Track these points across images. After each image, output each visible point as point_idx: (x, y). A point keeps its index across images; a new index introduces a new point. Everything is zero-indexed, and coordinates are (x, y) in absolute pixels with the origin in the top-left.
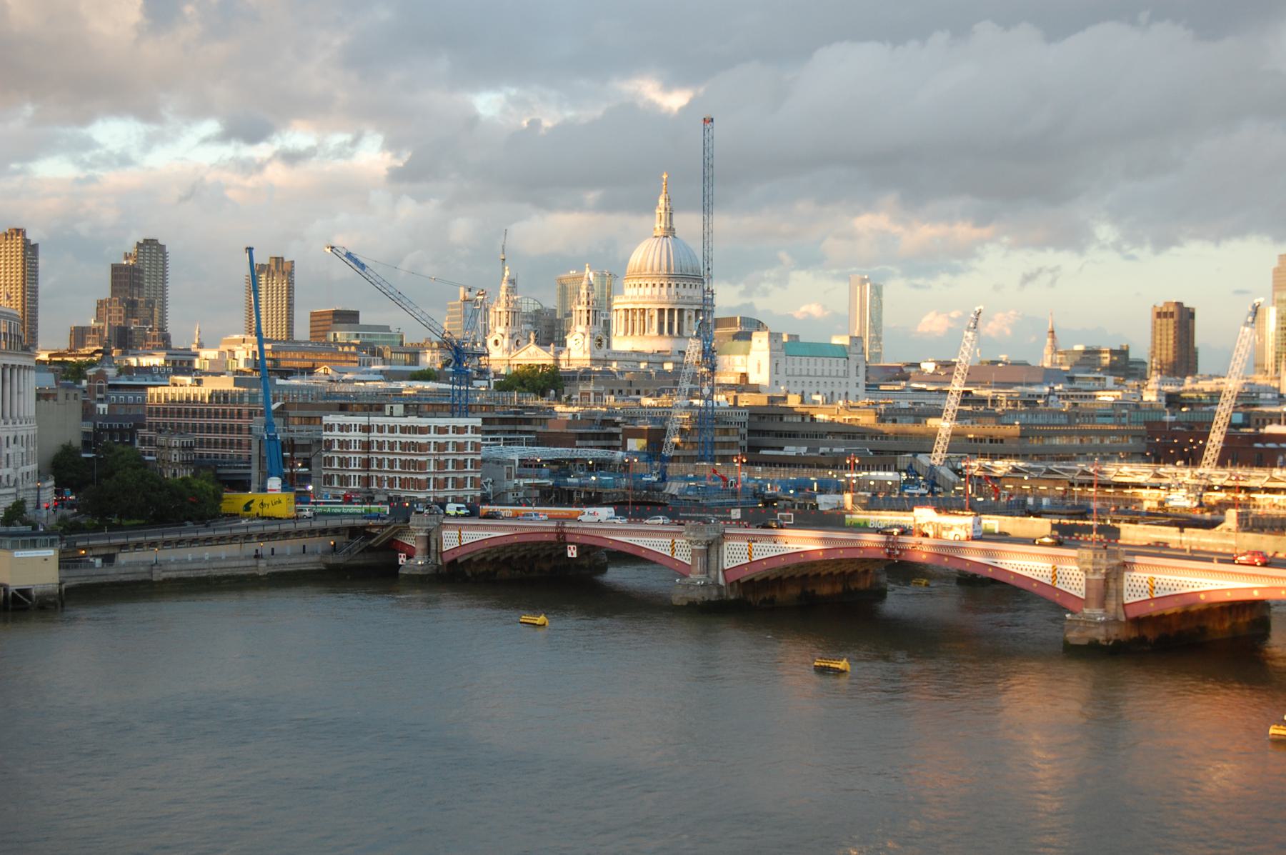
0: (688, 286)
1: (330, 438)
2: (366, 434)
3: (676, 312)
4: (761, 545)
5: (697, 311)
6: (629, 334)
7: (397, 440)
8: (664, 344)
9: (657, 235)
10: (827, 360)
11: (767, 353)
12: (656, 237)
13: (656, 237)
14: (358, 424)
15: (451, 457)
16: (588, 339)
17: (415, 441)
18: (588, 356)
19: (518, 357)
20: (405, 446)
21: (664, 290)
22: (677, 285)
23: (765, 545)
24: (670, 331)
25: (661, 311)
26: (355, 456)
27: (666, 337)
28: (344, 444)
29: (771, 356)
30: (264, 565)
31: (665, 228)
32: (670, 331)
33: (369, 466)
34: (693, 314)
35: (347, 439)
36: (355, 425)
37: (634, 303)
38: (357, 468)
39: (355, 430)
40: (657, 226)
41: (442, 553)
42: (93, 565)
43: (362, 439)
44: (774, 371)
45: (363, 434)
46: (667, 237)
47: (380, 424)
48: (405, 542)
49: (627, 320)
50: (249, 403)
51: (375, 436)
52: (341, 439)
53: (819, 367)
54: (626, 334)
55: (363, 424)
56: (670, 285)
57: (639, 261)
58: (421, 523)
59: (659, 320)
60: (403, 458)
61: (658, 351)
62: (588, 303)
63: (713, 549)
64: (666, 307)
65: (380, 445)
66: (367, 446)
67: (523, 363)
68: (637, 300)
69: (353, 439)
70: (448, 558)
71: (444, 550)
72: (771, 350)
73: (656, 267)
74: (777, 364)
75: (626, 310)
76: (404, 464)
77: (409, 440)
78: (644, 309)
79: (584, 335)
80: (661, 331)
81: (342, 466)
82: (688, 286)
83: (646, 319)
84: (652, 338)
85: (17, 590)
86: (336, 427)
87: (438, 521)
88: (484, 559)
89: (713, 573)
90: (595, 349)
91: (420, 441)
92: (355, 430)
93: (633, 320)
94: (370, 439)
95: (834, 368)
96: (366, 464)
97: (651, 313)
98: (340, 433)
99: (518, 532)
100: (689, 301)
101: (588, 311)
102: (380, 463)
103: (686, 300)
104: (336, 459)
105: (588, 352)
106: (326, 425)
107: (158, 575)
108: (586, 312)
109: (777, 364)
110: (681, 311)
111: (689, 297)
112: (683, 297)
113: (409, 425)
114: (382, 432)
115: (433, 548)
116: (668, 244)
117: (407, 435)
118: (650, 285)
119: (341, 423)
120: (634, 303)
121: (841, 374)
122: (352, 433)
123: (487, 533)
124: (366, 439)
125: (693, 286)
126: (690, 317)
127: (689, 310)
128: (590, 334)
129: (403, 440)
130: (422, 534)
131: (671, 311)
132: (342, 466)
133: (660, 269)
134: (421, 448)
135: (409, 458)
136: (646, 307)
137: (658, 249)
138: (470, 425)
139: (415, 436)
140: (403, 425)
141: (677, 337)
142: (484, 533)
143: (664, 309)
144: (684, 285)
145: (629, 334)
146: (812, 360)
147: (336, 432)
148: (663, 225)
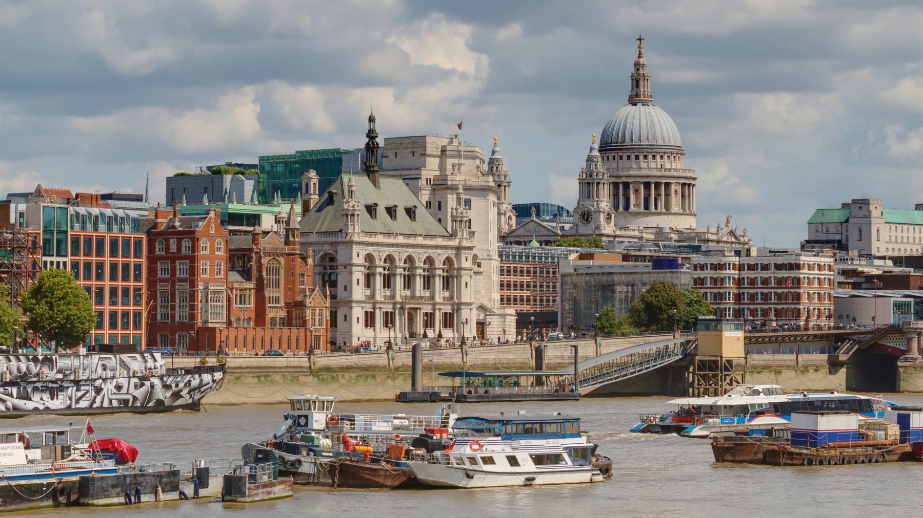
1: (702, 276)
3: (663, 186)
5: (684, 185)
25: (647, 185)
33: (740, 300)
34: (679, 188)
36: (729, 265)
39: (729, 269)
48: (888, 344)
51: (746, 274)
52: (715, 276)
65: (753, 282)
66: (739, 282)
69: (727, 276)
84: (637, 214)
85: (726, 360)
86: (709, 266)
94: (741, 277)
96: (738, 298)
98: (713, 272)
103: (673, 173)
110: (667, 185)
112: (669, 170)
113: (786, 262)
117: (784, 271)
119: (715, 263)
122: (728, 271)
126: (676, 191)
129: (780, 276)
146: (905, 227)
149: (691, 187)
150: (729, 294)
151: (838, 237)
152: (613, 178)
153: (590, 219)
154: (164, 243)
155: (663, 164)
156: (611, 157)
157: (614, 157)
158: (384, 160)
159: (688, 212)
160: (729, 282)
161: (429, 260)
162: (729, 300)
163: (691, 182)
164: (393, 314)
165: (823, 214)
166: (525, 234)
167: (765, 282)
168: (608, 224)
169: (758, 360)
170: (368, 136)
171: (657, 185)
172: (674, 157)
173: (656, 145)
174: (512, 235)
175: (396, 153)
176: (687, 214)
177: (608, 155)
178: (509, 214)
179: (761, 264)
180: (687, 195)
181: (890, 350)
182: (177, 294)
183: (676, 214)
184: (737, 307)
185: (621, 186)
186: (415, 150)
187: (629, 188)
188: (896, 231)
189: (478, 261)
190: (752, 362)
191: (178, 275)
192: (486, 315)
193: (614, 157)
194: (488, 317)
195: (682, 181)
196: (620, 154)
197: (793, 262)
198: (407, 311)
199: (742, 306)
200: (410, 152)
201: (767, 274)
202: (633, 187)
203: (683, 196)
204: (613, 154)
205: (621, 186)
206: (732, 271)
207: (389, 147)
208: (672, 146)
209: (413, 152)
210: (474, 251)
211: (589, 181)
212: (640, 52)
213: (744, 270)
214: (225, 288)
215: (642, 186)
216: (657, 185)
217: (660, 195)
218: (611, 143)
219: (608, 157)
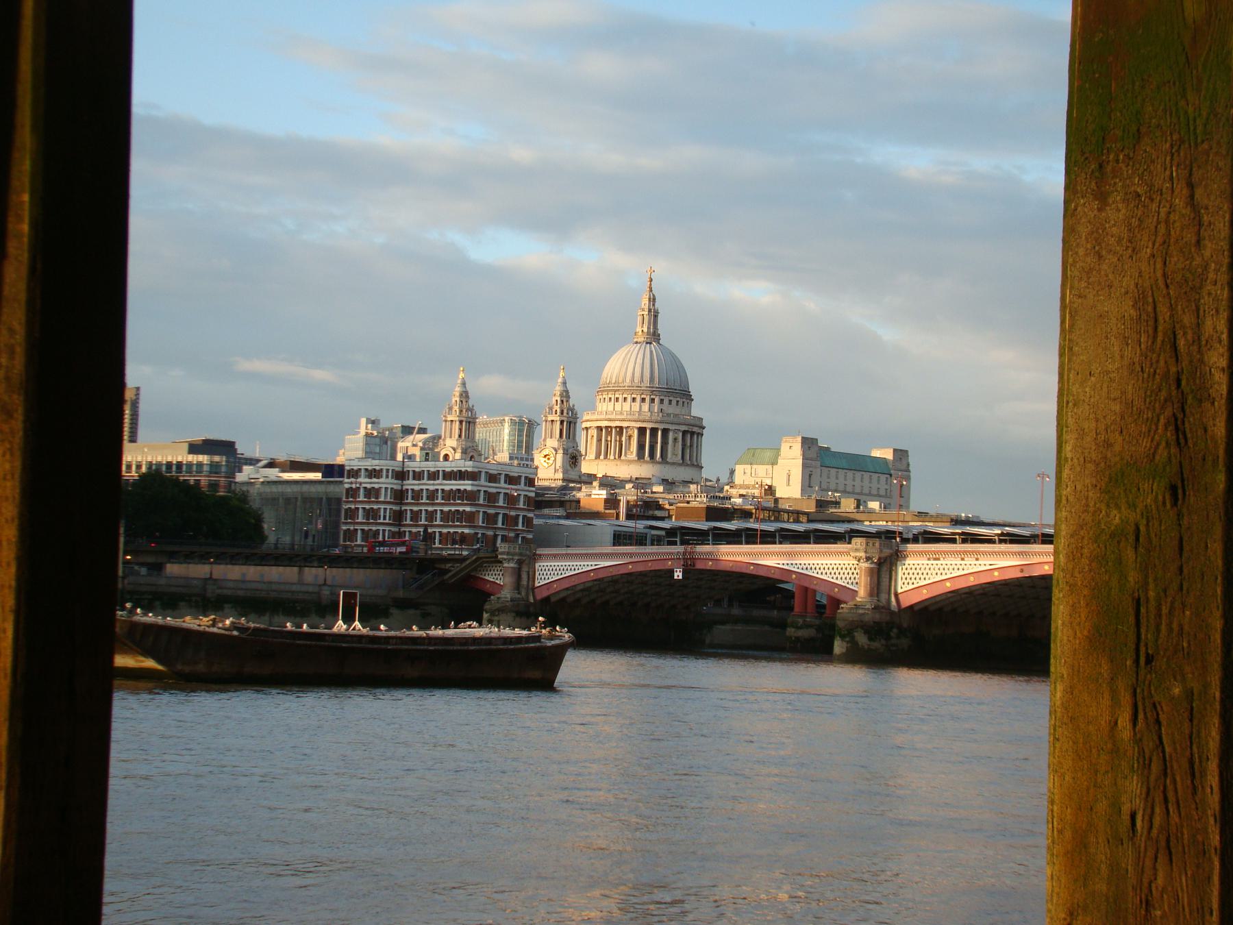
0: (674, 402)
2: (400, 482)
3: (660, 433)
4: (944, 562)
5: (684, 433)
6: (602, 457)
7: (440, 487)
8: (643, 470)
9: (639, 340)
10: (866, 475)
11: (800, 461)
12: (637, 343)
13: (637, 343)
14: (391, 468)
15: (502, 511)
16: (560, 456)
17: (462, 488)
18: (560, 475)
20: (450, 496)
21: (646, 407)
22: (662, 401)
23: (949, 563)
24: (652, 455)
25: (642, 431)
26: (385, 509)
27: (647, 462)
28: (372, 493)
29: (804, 466)
30: (328, 593)
31: (648, 333)
32: (652, 455)
35: (376, 486)
37: (610, 420)
38: (387, 521)
40: (639, 329)
41: (534, 588)
42: (138, 574)
43: (395, 487)
44: (807, 483)
45: (396, 481)
46: (650, 343)
47: (417, 470)
48: (487, 578)
49: (599, 440)
50: (211, 472)
51: (411, 484)
52: (369, 486)
53: (858, 483)
54: (598, 457)
55: (397, 469)
56: (653, 401)
57: (616, 371)
58: (512, 550)
59: (639, 441)
60: (446, 509)
61: (637, 479)
62: (562, 412)
63: (885, 568)
64: (649, 426)
65: (417, 495)
66: (399, 496)
68: (613, 417)
69: (384, 486)
70: (541, 595)
71: (537, 584)
72: (805, 458)
73: (638, 374)
74: (810, 475)
75: (600, 429)
76: (446, 516)
77: (454, 488)
78: (621, 428)
79: (556, 450)
80: (640, 455)
81: (368, 519)
82: (674, 402)
83: (623, 439)
84: (630, 462)
87: (530, 551)
88: (578, 600)
89: (883, 596)
90: (569, 468)
91: (469, 488)
92: (387, 477)
93: (607, 441)
94: (405, 487)
95: (875, 485)
96: (398, 517)
97: (630, 432)
98: (368, 480)
99: (634, 560)
100: (676, 420)
101: (562, 422)
102: (416, 516)
104: (361, 511)
105: (561, 470)
106: (349, 471)
107: (211, 591)
108: (559, 423)
109: (810, 475)
111: (676, 415)
112: (669, 415)
113: (455, 469)
114: (419, 480)
115: (524, 582)
116: (651, 352)
118: (629, 400)
119: (370, 468)
120: (610, 420)
121: (882, 492)
123: (593, 563)
124: (399, 487)
125: (681, 403)
126: (675, 440)
127: (676, 431)
128: (564, 449)
129: (447, 488)
130: (512, 565)
131: (654, 431)
132: (368, 519)
133: (642, 380)
134: (471, 497)
135: (453, 509)
136: (625, 424)
137: (641, 356)
138: (524, 475)
139: (462, 482)
140: (448, 470)
141: (659, 463)
142: (590, 563)
143: (645, 429)
144: (670, 401)
145: (602, 457)
146: (850, 474)
147: (363, 479)
148: (645, 330)
149: (695, 436)
150: (385, 512)
152: (606, 422)
155: (663, 408)
159: (689, 463)
160: (386, 495)
162: (385, 518)
163: (695, 429)
165: (753, 455)
167: (432, 495)
169: (233, 589)
172: (678, 402)
173: (657, 388)
176: (687, 465)
178: (471, 454)
179: (428, 471)
181: (488, 586)
183: (673, 464)
184: (394, 529)
188: (854, 480)
190: (219, 591)
193: (610, 398)
196: (617, 396)
197: (463, 469)
199: (403, 529)
201: (433, 485)
202: (627, 432)
204: (610, 396)
206: (390, 480)
208: (676, 390)
211: (553, 418)
212: (651, 284)
213: (408, 479)
215: (636, 431)
217: (657, 443)
218: (609, 384)
219: (605, 399)
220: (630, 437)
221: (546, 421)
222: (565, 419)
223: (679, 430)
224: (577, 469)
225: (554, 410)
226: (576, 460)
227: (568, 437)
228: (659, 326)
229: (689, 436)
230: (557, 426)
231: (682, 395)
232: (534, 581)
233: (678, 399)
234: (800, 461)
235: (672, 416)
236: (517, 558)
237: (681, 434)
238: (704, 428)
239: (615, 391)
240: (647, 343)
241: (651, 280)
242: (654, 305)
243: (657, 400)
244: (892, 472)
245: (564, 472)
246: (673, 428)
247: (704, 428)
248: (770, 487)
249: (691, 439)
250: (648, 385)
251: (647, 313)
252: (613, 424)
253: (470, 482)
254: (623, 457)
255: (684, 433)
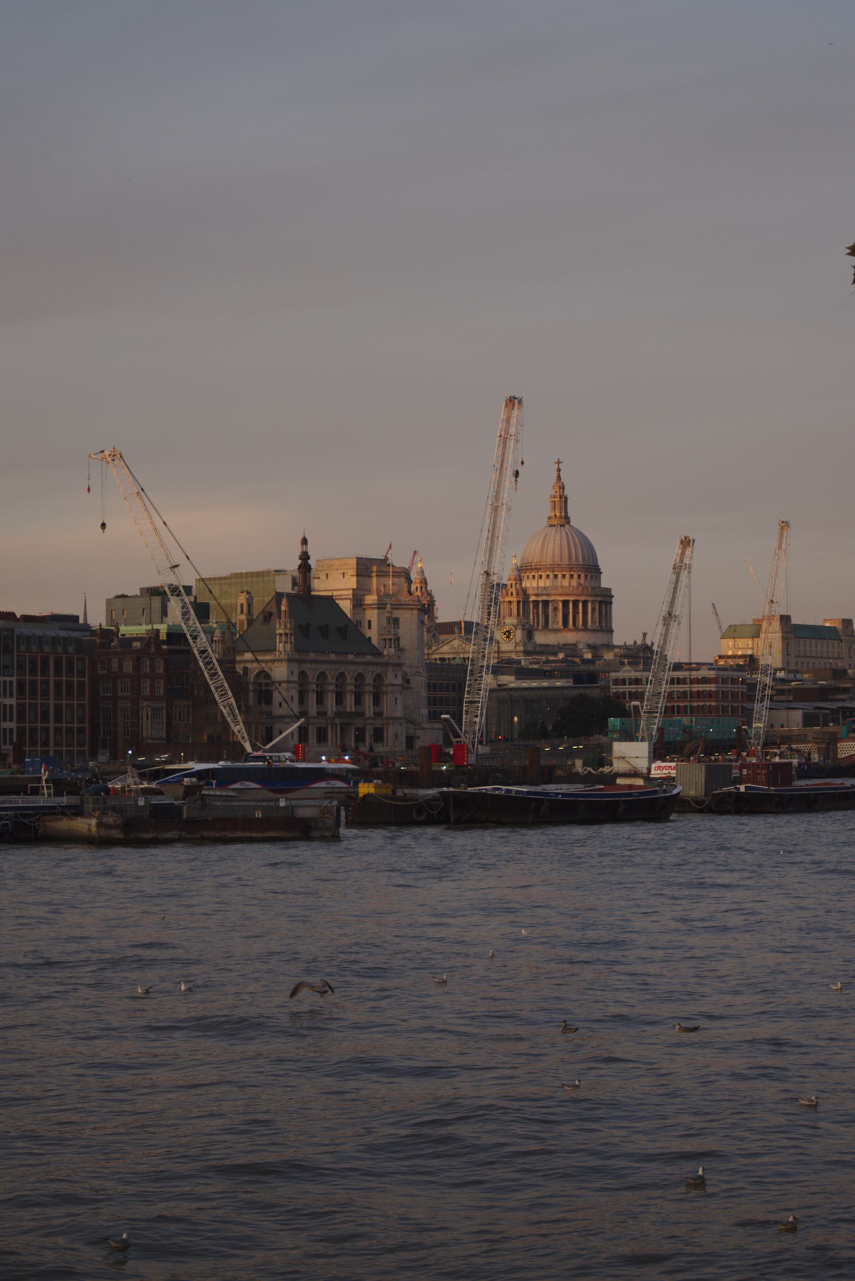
10: (825, 642)
19: (441, 650)
25: (565, 603)
29: (783, 638)
44: (785, 652)
46: (564, 526)
67: (446, 656)
84: (557, 631)
90: (527, 641)
91: (713, 689)
101: (518, 602)
108: (515, 603)
126: (593, 610)
130: (823, 746)
151: (749, 652)
153: (511, 637)
154: (106, 663)
156: (531, 577)
157: (534, 577)
158: (316, 581)
159: (605, 628)
161: (360, 677)
163: (608, 599)
164: (325, 729)
165: (735, 630)
166: (450, 651)
168: (529, 641)
170: (300, 558)
171: (576, 603)
172: (592, 576)
174: (436, 652)
175: (327, 574)
177: (528, 574)
178: (434, 632)
180: (604, 613)
182: (119, 711)
185: (540, 604)
186: (345, 571)
187: (549, 606)
189: (407, 677)
191: (120, 694)
192: (415, 729)
193: (534, 577)
194: (416, 731)
195: (599, 599)
196: (540, 573)
198: (339, 727)
200: (341, 574)
202: (553, 605)
203: (600, 614)
204: (533, 574)
205: (540, 604)
207: (320, 569)
209: (344, 573)
210: (404, 668)
211: (510, 599)
214: (165, 705)
215: (560, 605)
216: (576, 603)
217: (578, 613)
219: (528, 576)
220: (556, 609)
221: (504, 602)
222: (521, 599)
223: (596, 601)
224: (532, 642)
225: (510, 592)
226: (531, 633)
227: (524, 615)
228: (569, 511)
229: (604, 605)
230: (514, 607)
231: (592, 569)
232: (837, 755)
233: (592, 574)
234: (780, 635)
235: (590, 588)
236: (827, 741)
237: (597, 604)
238: (613, 597)
239: (539, 569)
240: (561, 526)
241: (559, 470)
242: (563, 492)
243: (575, 576)
244: (842, 638)
245: (525, 645)
246: (592, 599)
247: (613, 597)
248: (751, 656)
249: (606, 608)
250: (567, 563)
251: (558, 499)
252: (540, 599)
253: (714, 685)
254: (550, 627)
255: (601, 603)
